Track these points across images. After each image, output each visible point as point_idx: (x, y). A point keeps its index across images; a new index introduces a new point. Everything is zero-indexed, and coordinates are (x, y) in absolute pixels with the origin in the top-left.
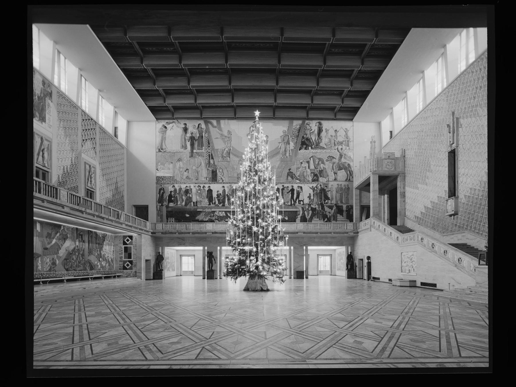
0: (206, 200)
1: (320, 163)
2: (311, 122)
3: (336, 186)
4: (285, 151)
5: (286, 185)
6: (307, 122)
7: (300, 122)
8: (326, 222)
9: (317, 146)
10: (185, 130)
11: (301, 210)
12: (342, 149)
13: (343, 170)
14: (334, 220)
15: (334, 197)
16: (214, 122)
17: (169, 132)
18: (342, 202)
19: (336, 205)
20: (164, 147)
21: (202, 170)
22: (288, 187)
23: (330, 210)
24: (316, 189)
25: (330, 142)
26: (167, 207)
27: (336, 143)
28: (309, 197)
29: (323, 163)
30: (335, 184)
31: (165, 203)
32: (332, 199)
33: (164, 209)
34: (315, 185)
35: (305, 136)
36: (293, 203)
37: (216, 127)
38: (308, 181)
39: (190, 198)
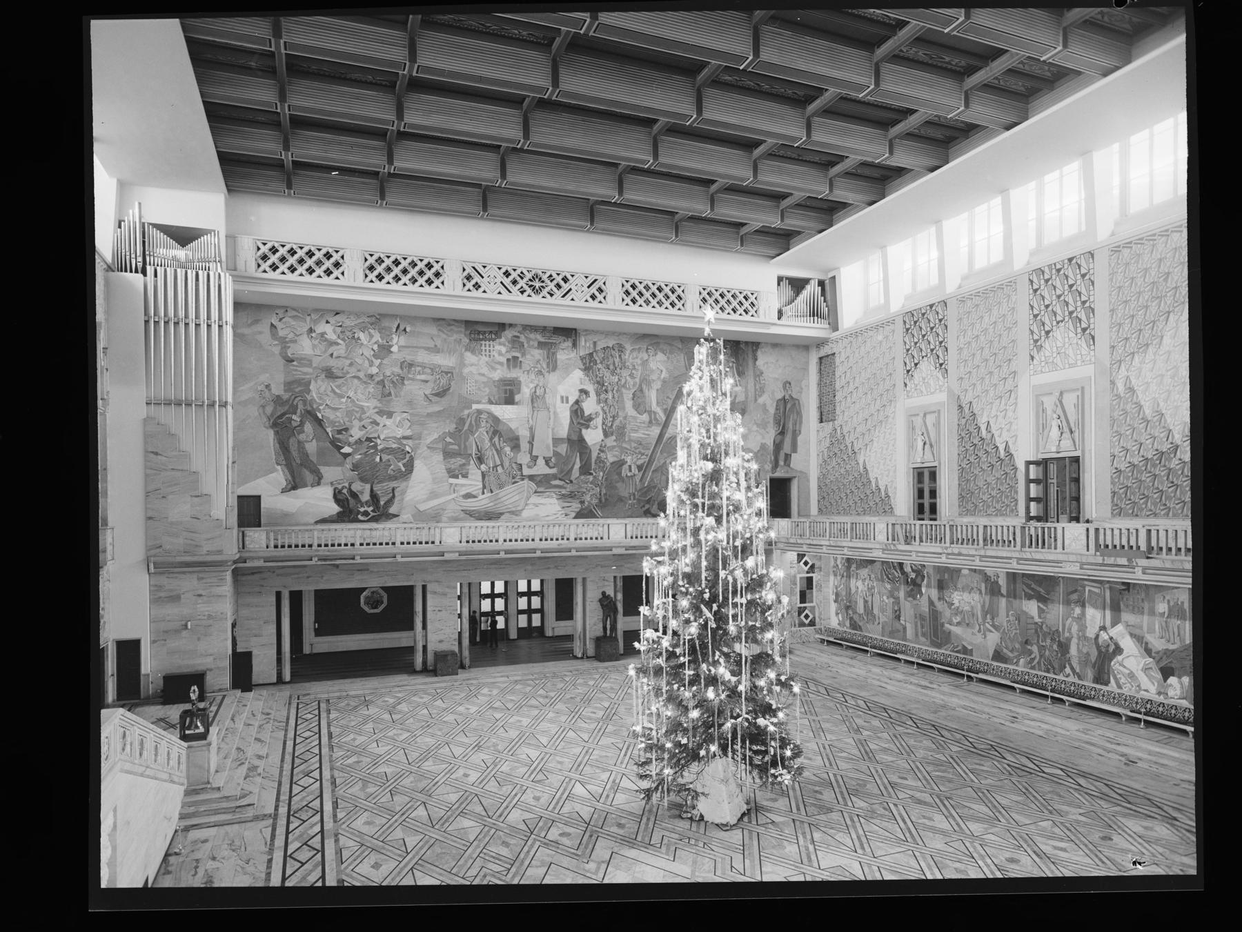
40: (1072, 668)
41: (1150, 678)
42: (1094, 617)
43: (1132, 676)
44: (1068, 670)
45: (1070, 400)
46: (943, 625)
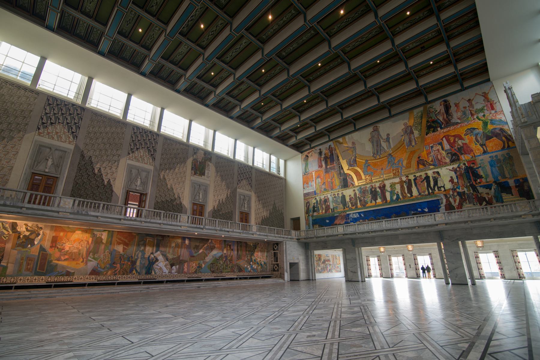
0: (341, 206)
1: (457, 140)
2: (433, 104)
3: (489, 159)
4: (410, 141)
5: (418, 175)
6: (429, 106)
7: (421, 109)
8: (486, 205)
9: (448, 123)
10: (320, 153)
11: (443, 197)
12: (484, 116)
13: (494, 138)
14: (497, 201)
15: (489, 172)
16: (341, 140)
17: (310, 159)
18: (504, 177)
19: (495, 182)
20: (307, 170)
21: (335, 180)
22: (421, 176)
23: (487, 191)
24: (458, 169)
25: (464, 113)
26: (312, 216)
27: (473, 112)
28: (452, 180)
29: (461, 138)
30: (487, 157)
31: (311, 213)
32: (487, 176)
33: (311, 219)
34: (455, 166)
35: (430, 120)
36: (431, 191)
37: (342, 143)
38: (446, 163)
39: (329, 206)
40: (136, 271)
41: (167, 268)
42: (149, 250)
43: (161, 269)
44: (134, 272)
45: (144, 174)
46: (51, 261)
